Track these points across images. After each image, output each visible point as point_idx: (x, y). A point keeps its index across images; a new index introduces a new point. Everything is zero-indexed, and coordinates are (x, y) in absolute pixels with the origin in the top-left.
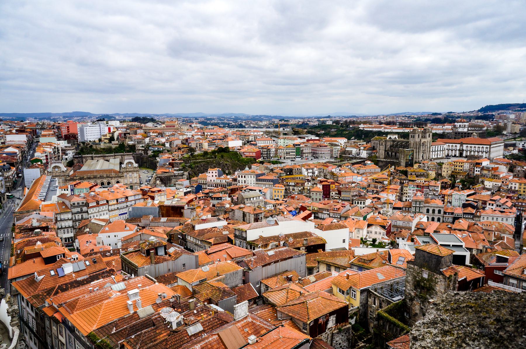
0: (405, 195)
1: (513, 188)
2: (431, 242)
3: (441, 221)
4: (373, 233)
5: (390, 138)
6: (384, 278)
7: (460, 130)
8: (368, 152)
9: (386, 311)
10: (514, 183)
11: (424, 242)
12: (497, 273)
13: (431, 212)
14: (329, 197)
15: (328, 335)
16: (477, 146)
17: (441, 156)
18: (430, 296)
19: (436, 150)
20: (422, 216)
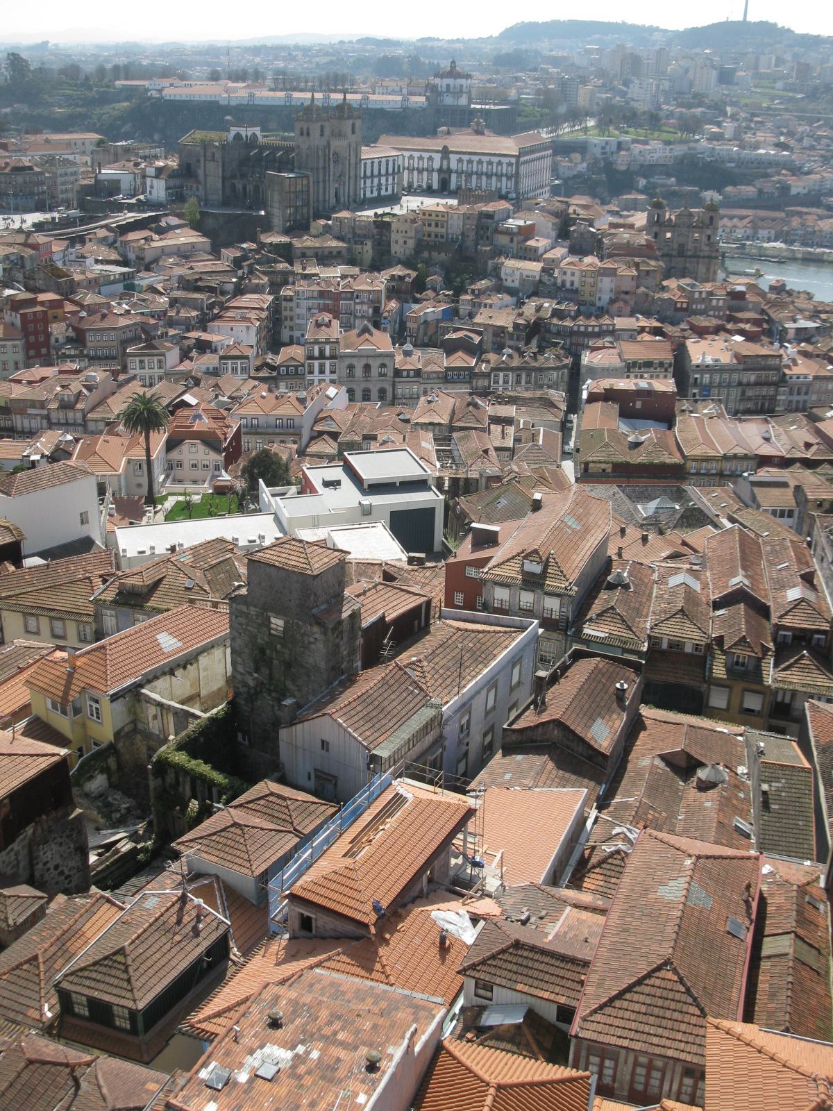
0: (288, 323)
1: (568, 285)
2: (346, 482)
3: (389, 396)
4: (186, 465)
5: (238, 136)
6: (180, 644)
7: (449, 100)
8: (171, 183)
9: (180, 747)
10: (569, 273)
11: (327, 484)
12: (471, 572)
13: (359, 372)
14: (48, 354)
15: (17, 854)
16: (485, 159)
17: (390, 192)
18: (293, 681)
19: (376, 172)
20: (332, 391)
